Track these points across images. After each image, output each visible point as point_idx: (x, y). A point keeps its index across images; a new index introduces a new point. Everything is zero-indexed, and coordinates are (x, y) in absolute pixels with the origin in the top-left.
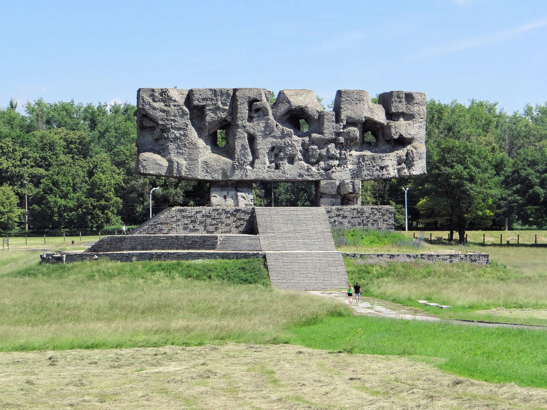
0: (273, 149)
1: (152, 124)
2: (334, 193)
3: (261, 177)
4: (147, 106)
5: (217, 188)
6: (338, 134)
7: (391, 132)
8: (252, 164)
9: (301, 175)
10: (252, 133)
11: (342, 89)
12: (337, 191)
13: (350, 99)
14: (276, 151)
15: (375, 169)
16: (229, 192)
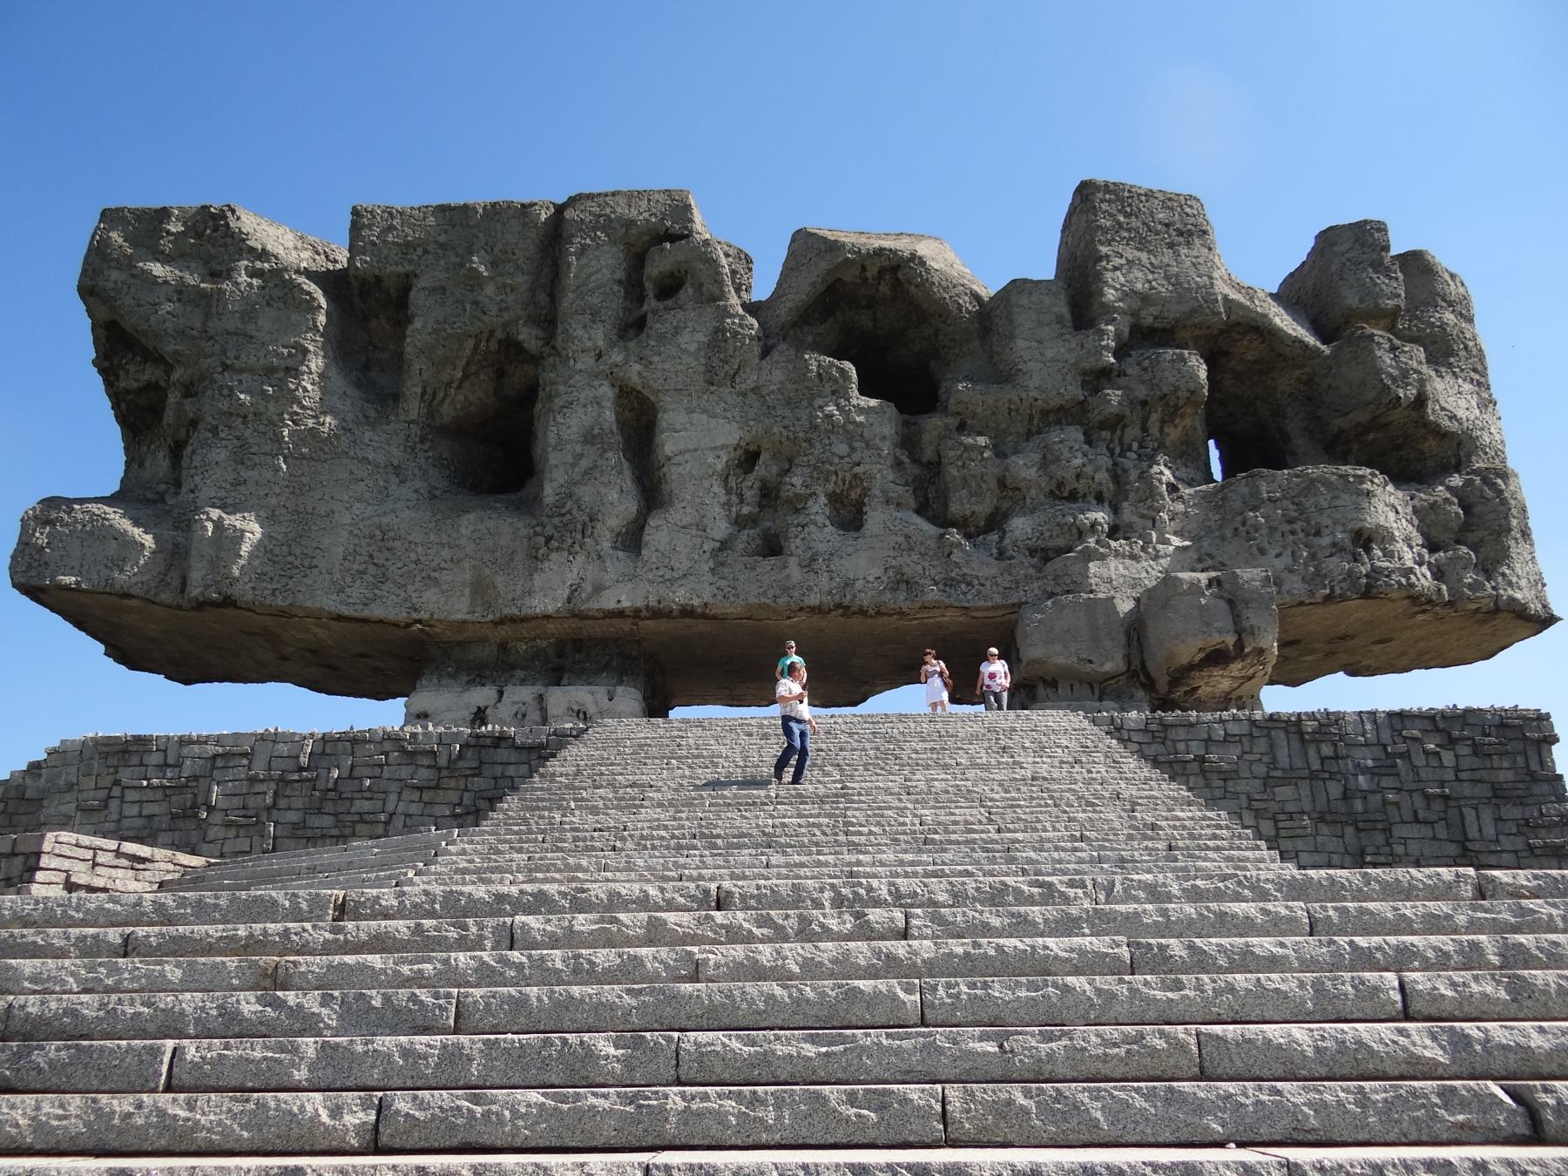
0: (749, 459)
1: (150, 373)
2: (1108, 667)
3: (680, 596)
4: (114, 275)
5: (453, 676)
6: (1099, 378)
7: (1379, 371)
8: (632, 539)
9: (901, 581)
10: (635, 380)
11: (1100, 176)
12: (1128, 658)
13: (1135, 223)
14: (766, 468)
15: (1325, 541)
16: (508, 689)
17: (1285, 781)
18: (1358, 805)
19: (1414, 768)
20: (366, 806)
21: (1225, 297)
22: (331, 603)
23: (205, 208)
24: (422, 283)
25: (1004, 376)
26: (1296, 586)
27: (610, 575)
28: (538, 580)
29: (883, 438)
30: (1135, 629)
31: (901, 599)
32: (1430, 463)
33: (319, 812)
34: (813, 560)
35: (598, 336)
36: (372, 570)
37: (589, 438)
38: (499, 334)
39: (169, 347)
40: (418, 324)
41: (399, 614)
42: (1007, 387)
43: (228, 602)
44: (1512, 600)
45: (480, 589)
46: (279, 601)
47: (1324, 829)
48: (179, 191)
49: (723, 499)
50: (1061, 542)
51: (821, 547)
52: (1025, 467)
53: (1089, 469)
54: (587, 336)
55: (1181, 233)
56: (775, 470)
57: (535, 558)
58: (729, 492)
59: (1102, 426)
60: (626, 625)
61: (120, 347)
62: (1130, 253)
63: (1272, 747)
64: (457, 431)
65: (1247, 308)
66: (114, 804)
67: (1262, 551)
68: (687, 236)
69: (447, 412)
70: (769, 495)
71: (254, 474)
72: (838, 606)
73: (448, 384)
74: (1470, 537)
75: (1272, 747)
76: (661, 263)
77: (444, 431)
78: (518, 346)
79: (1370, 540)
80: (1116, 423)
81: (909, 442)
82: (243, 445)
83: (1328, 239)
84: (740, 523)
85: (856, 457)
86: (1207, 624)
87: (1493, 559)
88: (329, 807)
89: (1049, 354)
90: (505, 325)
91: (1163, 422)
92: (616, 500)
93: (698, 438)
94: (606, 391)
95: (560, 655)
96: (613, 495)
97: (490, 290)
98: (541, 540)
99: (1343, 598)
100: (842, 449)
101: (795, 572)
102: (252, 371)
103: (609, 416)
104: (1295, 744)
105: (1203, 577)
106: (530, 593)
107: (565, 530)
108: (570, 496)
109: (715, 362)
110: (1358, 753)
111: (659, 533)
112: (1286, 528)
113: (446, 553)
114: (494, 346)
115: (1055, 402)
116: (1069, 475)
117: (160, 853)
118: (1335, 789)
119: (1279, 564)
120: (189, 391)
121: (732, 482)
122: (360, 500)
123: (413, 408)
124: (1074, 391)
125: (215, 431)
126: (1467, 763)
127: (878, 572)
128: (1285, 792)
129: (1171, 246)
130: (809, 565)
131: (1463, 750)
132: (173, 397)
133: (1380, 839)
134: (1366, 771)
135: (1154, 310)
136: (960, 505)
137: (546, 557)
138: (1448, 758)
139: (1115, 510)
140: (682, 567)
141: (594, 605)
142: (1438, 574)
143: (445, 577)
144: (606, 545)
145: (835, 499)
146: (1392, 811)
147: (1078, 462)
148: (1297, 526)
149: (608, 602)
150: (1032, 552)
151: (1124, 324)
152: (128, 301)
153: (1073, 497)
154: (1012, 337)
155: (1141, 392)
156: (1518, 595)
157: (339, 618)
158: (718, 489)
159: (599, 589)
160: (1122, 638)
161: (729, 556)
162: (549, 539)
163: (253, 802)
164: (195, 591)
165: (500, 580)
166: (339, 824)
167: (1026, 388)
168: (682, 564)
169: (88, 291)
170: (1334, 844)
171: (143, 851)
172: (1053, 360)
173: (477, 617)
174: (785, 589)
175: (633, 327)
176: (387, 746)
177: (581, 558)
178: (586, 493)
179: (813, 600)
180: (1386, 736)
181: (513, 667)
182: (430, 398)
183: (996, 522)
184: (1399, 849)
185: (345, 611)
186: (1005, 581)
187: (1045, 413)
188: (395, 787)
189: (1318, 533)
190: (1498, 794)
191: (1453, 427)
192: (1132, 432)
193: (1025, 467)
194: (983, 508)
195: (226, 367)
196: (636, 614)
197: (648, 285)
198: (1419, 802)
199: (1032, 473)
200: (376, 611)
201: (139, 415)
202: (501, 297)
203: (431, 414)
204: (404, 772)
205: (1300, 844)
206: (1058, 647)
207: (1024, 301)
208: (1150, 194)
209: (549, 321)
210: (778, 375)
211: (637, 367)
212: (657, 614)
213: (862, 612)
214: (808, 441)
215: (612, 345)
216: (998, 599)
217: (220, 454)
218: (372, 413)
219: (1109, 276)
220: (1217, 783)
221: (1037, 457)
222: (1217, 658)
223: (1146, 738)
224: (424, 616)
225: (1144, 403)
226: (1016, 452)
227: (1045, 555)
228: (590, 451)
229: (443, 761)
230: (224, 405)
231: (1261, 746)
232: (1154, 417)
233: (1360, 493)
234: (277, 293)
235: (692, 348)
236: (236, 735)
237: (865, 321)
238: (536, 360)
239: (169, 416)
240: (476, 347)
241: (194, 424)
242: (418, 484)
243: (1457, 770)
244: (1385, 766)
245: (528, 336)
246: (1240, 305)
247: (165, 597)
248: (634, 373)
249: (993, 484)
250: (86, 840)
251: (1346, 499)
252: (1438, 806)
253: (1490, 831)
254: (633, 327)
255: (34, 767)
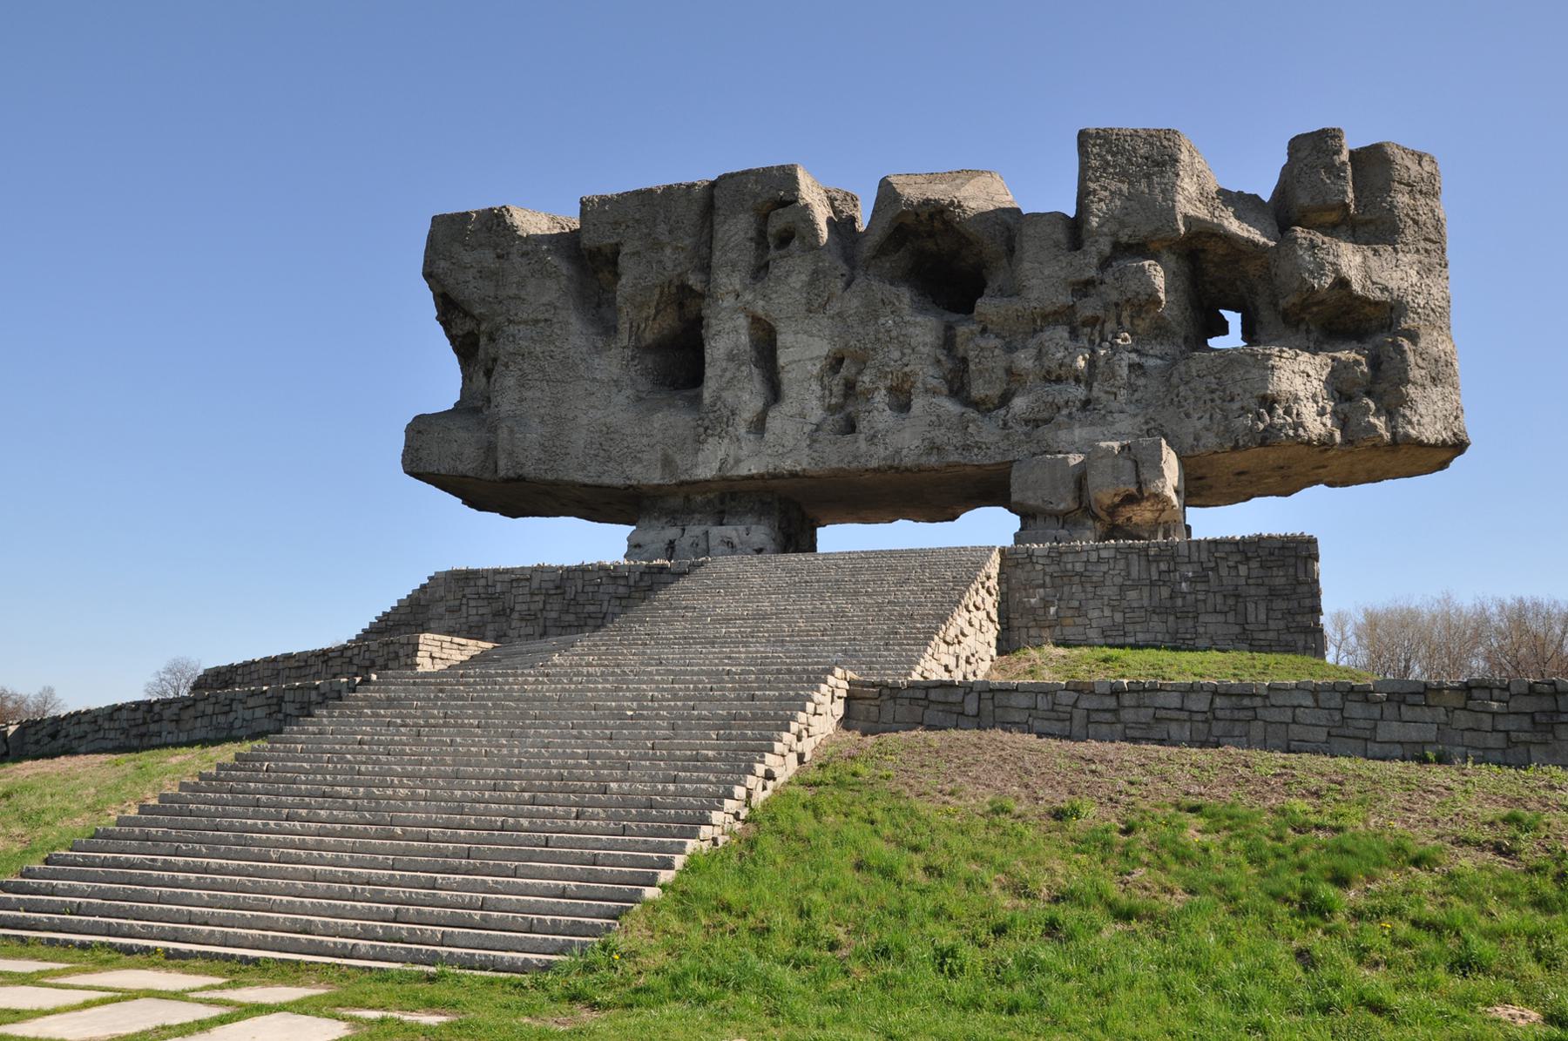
0: (836, 363)
1: (469, 325)
2: (1062, 506)
3: (788, 465)
4: (442, 264)
5: (657, 519)
8: (759, 426)
9: (934, 448)
10: (760, 313)
11: (1092, 125)
14: (847, 370)
15: (1236, 406)
17: (1134, 587)
18: (1179, 602)
19: (1220, 578)
20: (592, 608)
21: (1186, 216)
22: (579, 477)
23: (491, 210)
24: (625, 250)
25: (1015, 292)
26: (1210, 440)
27: (744, 452)
28: (700, 457)
29: (925, 345)
30: (1080, 480)
31: (933, 460)
32: (1374, 323)
33: (567, 612)
34: (874, 436)
35: (736, 282)
36: (602, 453)
37: (731, 357)
38: (676, 282)
39: (478, 310)
40: (623, 281)
41: (618, 481)
42: (1015, 299)
43: (520, 479)
44: (1407, 435)
45: (667, 462)
46: (549, 477)
47: (1155, 618)
48: (473, 202)
49: (819, 393)
50: (1045, 415)
51: (881, 426)
52: (1024, 360)
53: (1067, 360)
54: (729, 280)
55: (1157, 164)
56: (853, 370)
57: (699, 441)
58: (823, 388)
59: (1084, 324)
60: (760, 483)
61: (449, 309)
62: (1114, 185)
63: (1128, 565)
64: (658, 347)
65: (1204, 221)
66: (464, 608)
67: (1188, 415)
68: (792, 202)
69: (649, 337)
70: (850, 387)
71: (529, 394)
72: (891, 467)
73: (647, 319)
74: (1379, 388)
75: (1128, 565)
76: (777, 223)
77: (648, 349)
78: (690, 289)
79: (1275, 401)
80: (1093, 322)
81: (948, 342)
82: (524, 375)
83: (1296, 145)
84: (831, 409)
85: (905, 360)
86: (1117, 478)
87: (1393, 406)
88: (572, 609)
89: (1046, 273)
90: (679, 275)
91: (1132, 317)
92: (750, 399)
93: (803, 351)
94: (742, 321)
95: (722, 502)
96: (746, 397)
97: (668, 251)
98: (701, 430)
99: (1246, 447)
100: (896, 355)
101: (863, 445)
102: (526, 322)
103: (744, 339)
104: (1143, 563)
105: (1116, 445)
106: (696, 465)
107: (713, 424)
108: (719, 398)
109: (812, 296)
110: (1183, 568)
111: (775, 422)
112: (1208, 397)
113: (645, 440)
114: (673, 290)
115: (1050, 309)
116: (1054, 365)
117: (471, 642)
118: (1165, 592)
119: (1199, 425)
120: (492, 339)
121: (826, 380)
122: (593, 407)
123: (624, 337)
124: (1065, 299)
125: (506, 366)
126: (1255, 573)
127: (917, 442)
128: (1132, 595)
129: (1148, 176)
130: (872, 439)
131: (1254, 564)
132: (483, 340)
133: (1190, 623)
134: (1187, 579)
135: (1128, 231)
136: (978, 390)
137: (705, 441)
138: (1243, 570)
139: (1089, 386)
140: (790, 443)
141: (734, 473)
142: (1343, 421)
143: (645, 456)
144: (742, 431)
145: (891, 390)
146: (1201, 605)
147: (1059, 355)
148: (1215, 396)
149: (743, 471)
150: (1027, 422)
151: (1105, 246)
152: (451, 281)
153: (1059, 380)
154: (1021, 260)
155: (1114, 296)
156: (1413, 433)
157: (585, 485)
158: (815, 386)
159: (738, 461)
160: (1072, 485)
161: (821, 435)
162: (706, 429)
163: (533, 607)
164: (502, 473)
165: (678, 458)
166: (578, 618)
167: (1028, 301)
168: (790, 443)
169: (428, 275)
170: (1160, 627)
171: (463, 641)
172: (1049, 277)
173: (667, 481)
174: (855, 457)
175: (760, 271)
176: (602, 574)
177: (726, 441)
178: (728, 396)
179: (874, 464)
180: (1204, 556)
181: (693, 512)
182: (636, 332)
183: (1005, 399)
184: (1201, 630)
185: (587, 481)
186: (1004, 445)
187: (1045, 317)
188: (607, 597)
189: (1232, 400)
190: (1273, 593)
191: (1385, 297)
192: (1110, 326)
193: (1024, 360)
194: (995, 392)
195: (510, 322)
196: (762, 476)
197: (770, 239)
198: (1219, 600)
199: (1030, 364)
200: (606, 480)
201: (465, 348)
202: (673, 261)
203: (638, 340)
204: (611, 589)
205: (1138, 627)
206: (1030, 494)
207: (1031, 231)
208: (1135, 134)
209: (706, 268)
210: (855, 303)
211: (761, 303)
212: (774, 476)
213: (907, 469)
214: (874, 349)
215: (745, 287)
216: (999, 459)
217: (510, 382)
218: (600, 344)
219: (1094, 206)
220: (1090, 589)
221: (1033, 352)
222: (1130, 500)
223: (1048, 561)
224: (634, 482)
225: (1117, 305)
226: (1024, 347)
227: (1037, 423)
228: (732, 366)
229: (632, 582)
230: (511, 348)
231: (1121, 564)
232: (1125, 314)
233: (1266, 368)
234: (537, 267)
235: (798, 286)
236: (523, 568)
237: (930, 245)
238: (702, 296)
239: (481, 354)
240: (662, 293)
241: (495, 360)
242: (629, 392)
243: (1248, 577)
244: (1201, 577)
245: (694, 281)
246: (1197, 219)
247: (487, 476)
248: (759, 307)
249: (1001, 373)
250: (437, 637)
251: (1255, 373)
252: (1231, 602)
253: (1262, 617)
254: (760, 271)
255: (423, 587)
